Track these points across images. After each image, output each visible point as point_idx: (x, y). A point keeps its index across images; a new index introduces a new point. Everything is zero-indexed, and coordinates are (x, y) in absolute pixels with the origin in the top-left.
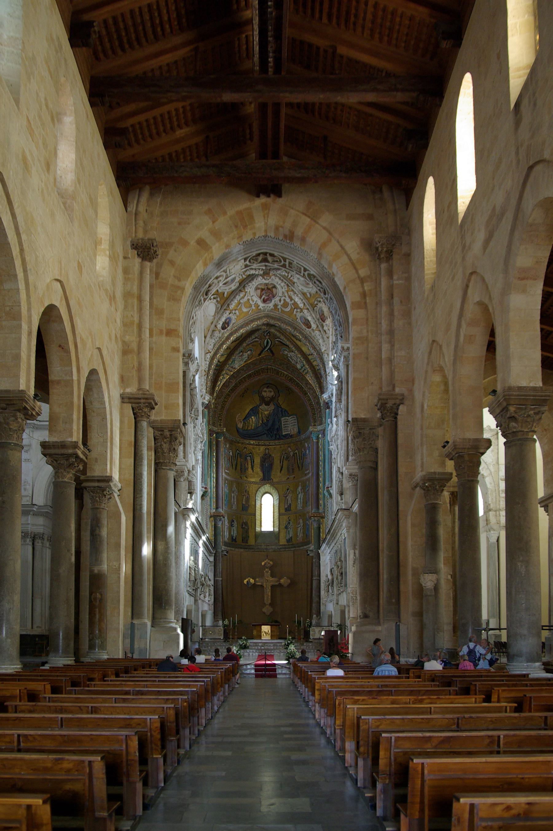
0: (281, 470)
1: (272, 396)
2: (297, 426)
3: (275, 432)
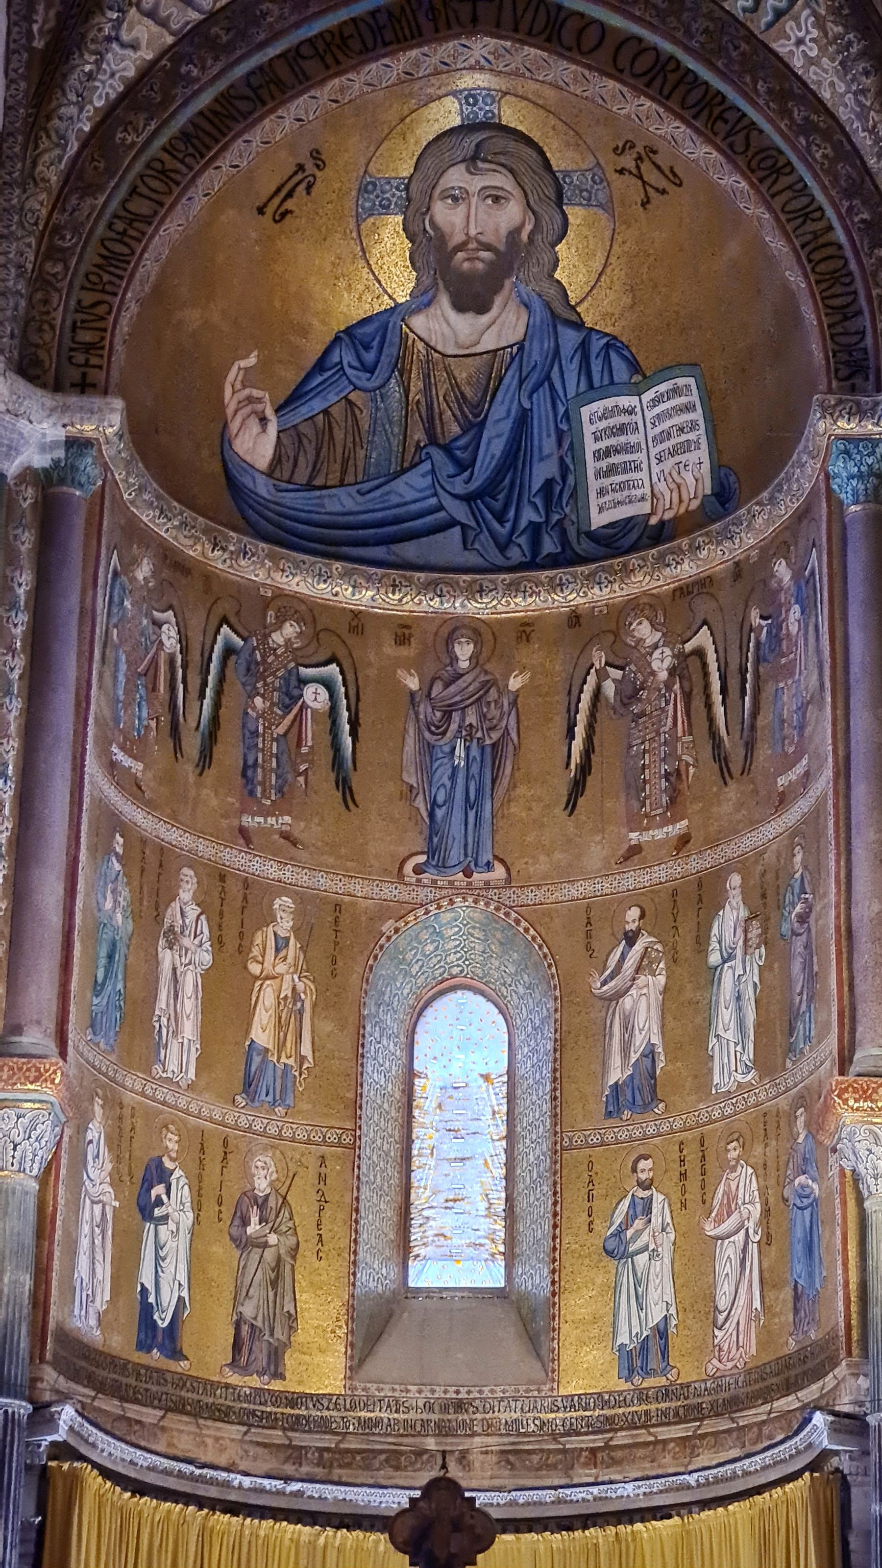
0: (578, 787)
1: (515, 233)
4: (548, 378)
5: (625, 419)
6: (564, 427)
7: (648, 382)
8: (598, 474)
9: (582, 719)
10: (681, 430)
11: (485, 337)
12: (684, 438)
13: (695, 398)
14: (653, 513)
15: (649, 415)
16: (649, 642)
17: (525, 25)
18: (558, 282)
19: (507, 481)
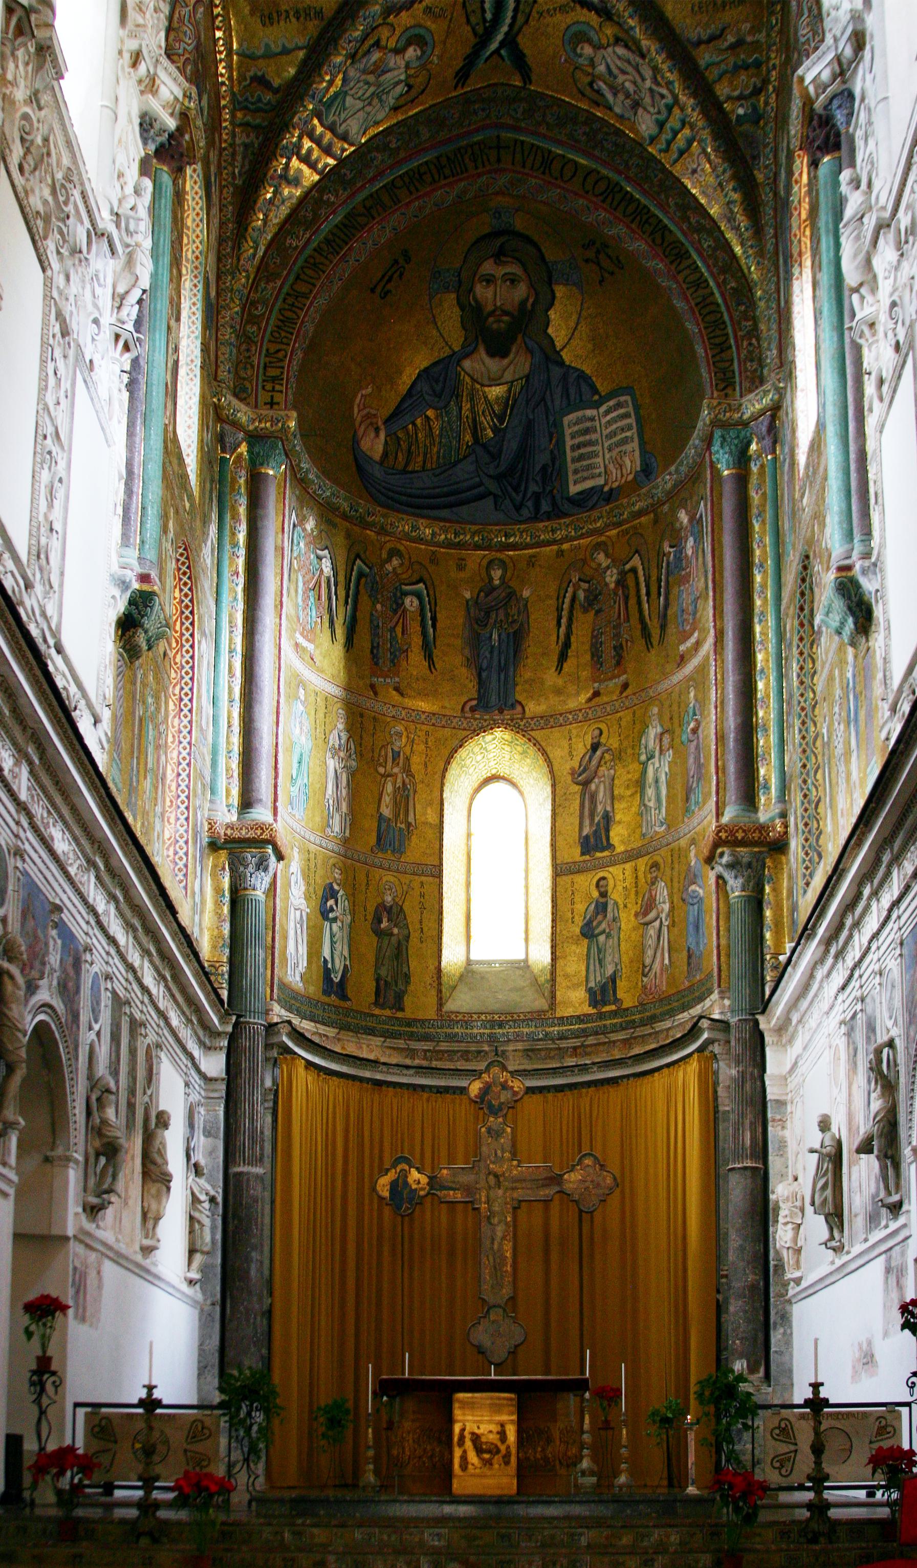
2: (635, 445)
3: (533, 488)
4: (543, 399)
5: (589, 424)
6: (552, 430)
7: (603, 400)
8: (574, 461)
9: (565, 613)
10: (622, 430)
11: (506, 373)
12: (623, 435)
13: (630, 409)
14: (606, 484)
15: (604, 421)
16: (604, 565)
17: (529, 164)
18: (549, 336)
19: (520, 466)
